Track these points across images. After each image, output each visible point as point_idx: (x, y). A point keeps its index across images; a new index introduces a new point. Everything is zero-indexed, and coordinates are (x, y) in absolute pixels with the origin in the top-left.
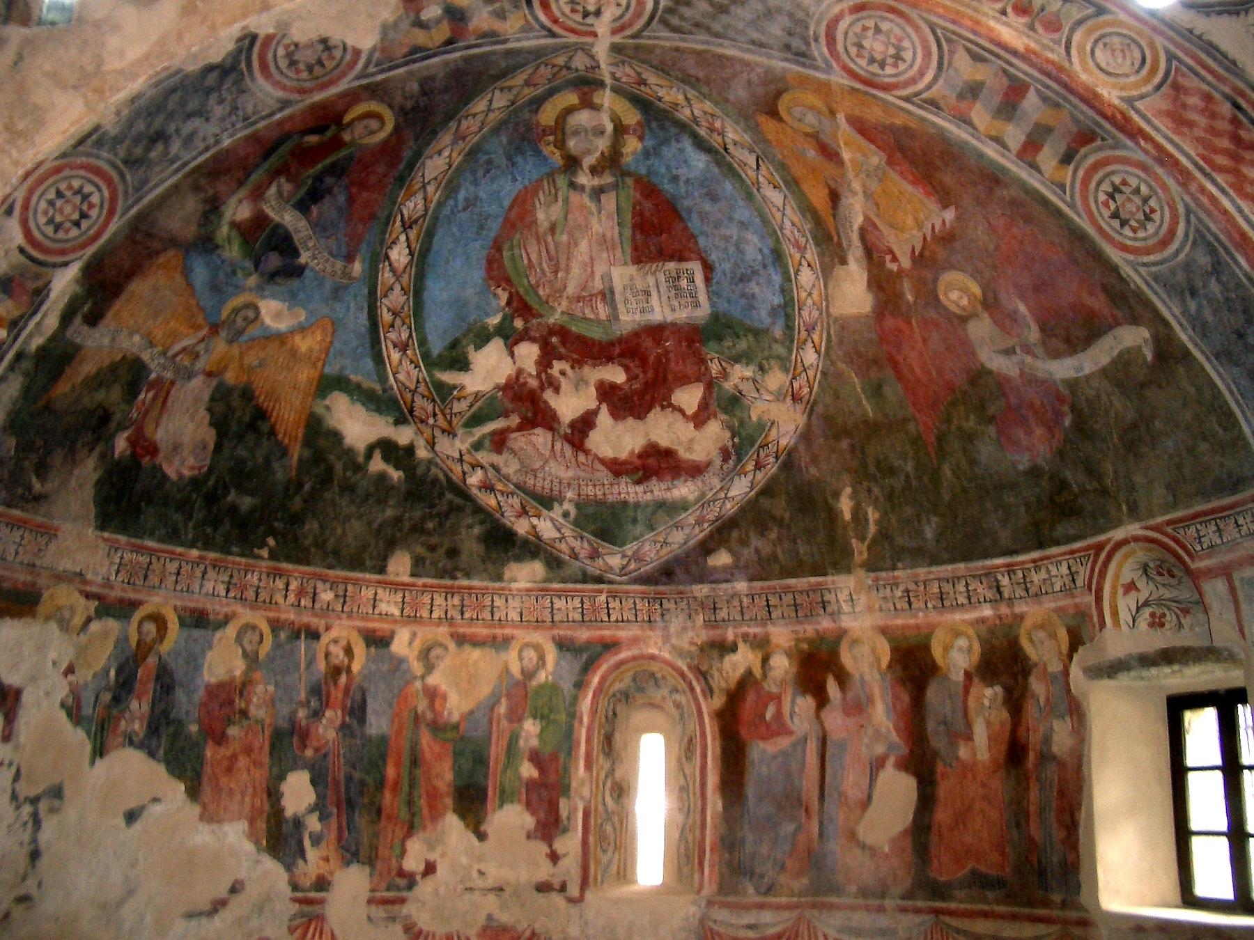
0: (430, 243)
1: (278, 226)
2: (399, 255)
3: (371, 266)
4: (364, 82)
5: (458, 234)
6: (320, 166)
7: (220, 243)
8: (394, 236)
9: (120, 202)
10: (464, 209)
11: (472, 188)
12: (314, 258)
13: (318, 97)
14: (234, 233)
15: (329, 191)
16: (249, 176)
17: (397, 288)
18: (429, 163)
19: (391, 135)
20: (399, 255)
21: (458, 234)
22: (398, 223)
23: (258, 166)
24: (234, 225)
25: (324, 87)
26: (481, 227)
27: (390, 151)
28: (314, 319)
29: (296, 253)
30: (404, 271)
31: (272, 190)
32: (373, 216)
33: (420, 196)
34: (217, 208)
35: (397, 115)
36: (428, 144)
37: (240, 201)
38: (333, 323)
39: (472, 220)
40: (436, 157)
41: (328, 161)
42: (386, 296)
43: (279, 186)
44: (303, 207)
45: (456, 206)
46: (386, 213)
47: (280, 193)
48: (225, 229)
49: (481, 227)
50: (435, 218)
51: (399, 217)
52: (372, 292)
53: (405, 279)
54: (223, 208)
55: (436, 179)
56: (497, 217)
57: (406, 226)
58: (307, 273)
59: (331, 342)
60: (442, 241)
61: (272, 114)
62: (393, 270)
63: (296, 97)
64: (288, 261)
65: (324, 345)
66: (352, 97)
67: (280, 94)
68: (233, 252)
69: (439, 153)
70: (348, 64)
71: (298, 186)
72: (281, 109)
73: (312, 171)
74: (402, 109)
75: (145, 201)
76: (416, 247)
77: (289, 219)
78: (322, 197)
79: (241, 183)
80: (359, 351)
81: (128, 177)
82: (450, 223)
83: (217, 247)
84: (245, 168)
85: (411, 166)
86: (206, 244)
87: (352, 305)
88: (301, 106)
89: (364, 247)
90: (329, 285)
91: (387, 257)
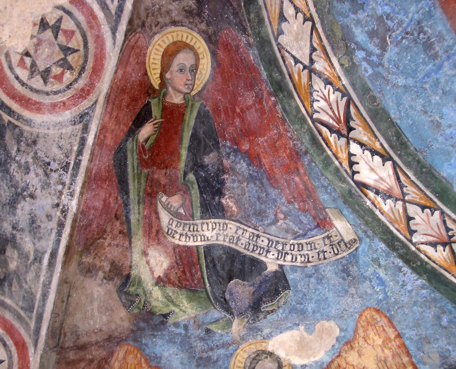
0: (393, 124)
1: (208, 249)
2: (373, 171)
3: (354, 211)
4: (123, 27)
5: (410, 82)
6: (184, 153)
7: (165, 311)
8: (343, 156)
9: (22, 332)
10: (383, 47)
11: (361, 16)
12: (282, 254)
13: (104, 85)
14: (170, 290)
15: (222, 170)
16: (128, 222)
17: (413, 210)
18: (283, 39)
19: (214, 54)
20: (373, 171)
21: (410, 82)
22: (332, 138)
23: (126, 205)
24: (160, 282)
25: (97, 70)
26: (428, 46)
27: (231, 70)
28: (352, 325)
29: (257, 265)
30: (402, 187)
31: (165, 218)
32: (296, 155)
33: (318, 84)
34: (128, 277)
35: (192, 26)
36: (261, 21)
37: (145, 254)
38: (378, 311)
39: (407, 48)
40: (284, 25)
41: (186, 142)
42: (412, 232)
43: (167, 208)
44: (212, 207)
45: (369, 54)
46: (306, 139)
47: (176, 215)
48: (157, 294)
49: (428, 46)
50: (364, 92)
51: (324, 130)
52: (391, 241)
53: (412, 193)
54: (134, 273)
55: (313, 49)
56: (430, 15)
57: (345, 130)
58: (290, 277)
59: (399, 336)
60: (404, 110)
61: (83, 142)
62: (387, 195)
63: (85, 104)
64: (257, 280)
65: (394, 344)
66: (132, 52)
67: (68, 115)
68: (186, 310)
69: (282, 18)
70: (89, 22)
71: (186, 191)
72: (86, 129)
73: (182, 165)
74: (189, 13)
75: (47, 316)
76: (380, 143)
77: (212, 233)
78: (222, 183)
79: (127, 234)
80: (445, 321)
81: (8, 301)
82: (387, 81)
83: (166, 316)
84: (117, 217)
85: (271, 63)
86: (151, 321)
87: (381, 273)
88: (99, 110)
89: (323, 197)
90: (329, 271)
91: (362, 186)
